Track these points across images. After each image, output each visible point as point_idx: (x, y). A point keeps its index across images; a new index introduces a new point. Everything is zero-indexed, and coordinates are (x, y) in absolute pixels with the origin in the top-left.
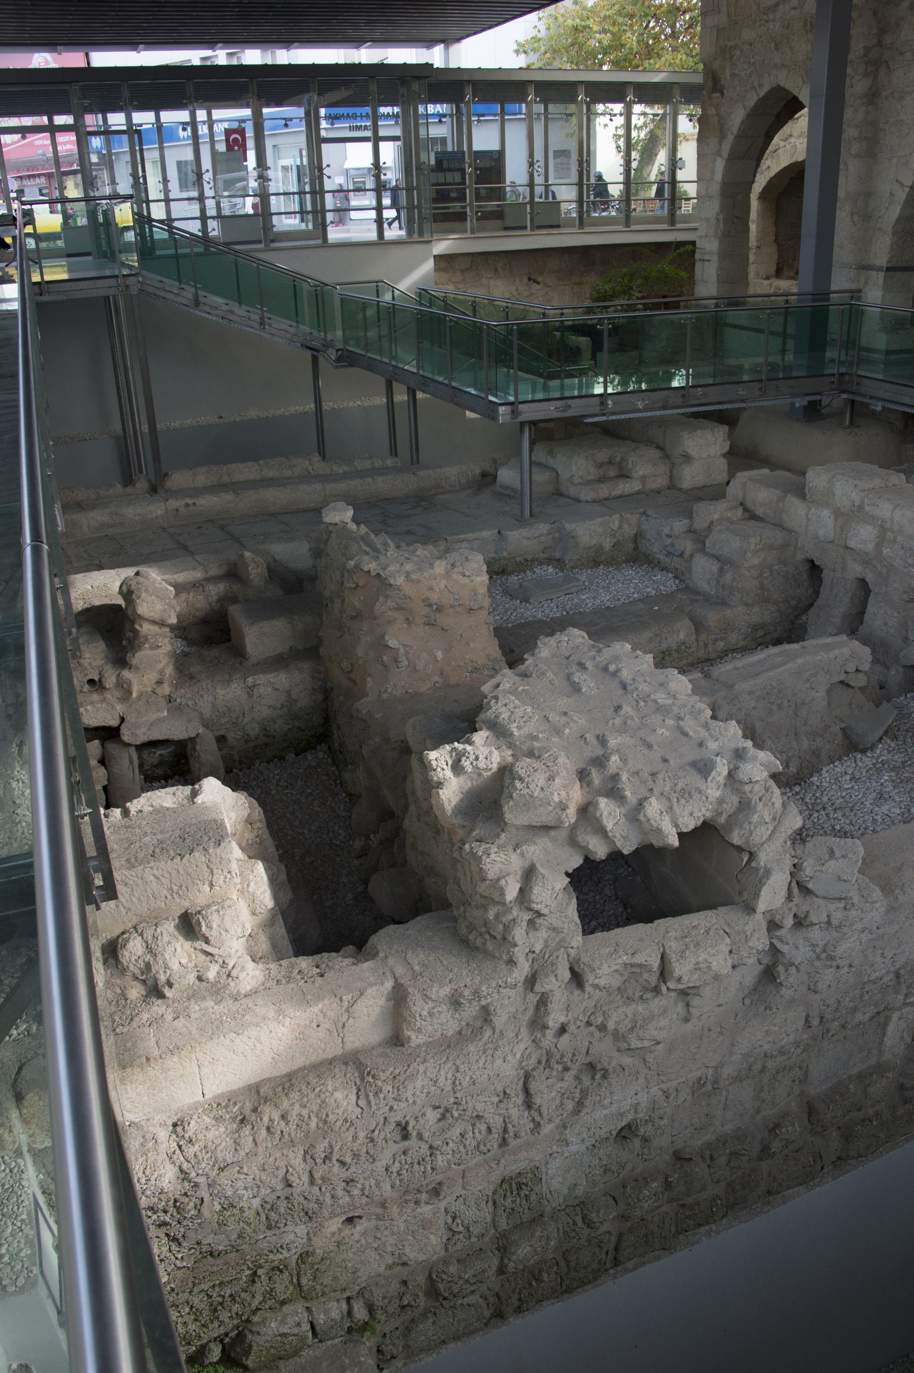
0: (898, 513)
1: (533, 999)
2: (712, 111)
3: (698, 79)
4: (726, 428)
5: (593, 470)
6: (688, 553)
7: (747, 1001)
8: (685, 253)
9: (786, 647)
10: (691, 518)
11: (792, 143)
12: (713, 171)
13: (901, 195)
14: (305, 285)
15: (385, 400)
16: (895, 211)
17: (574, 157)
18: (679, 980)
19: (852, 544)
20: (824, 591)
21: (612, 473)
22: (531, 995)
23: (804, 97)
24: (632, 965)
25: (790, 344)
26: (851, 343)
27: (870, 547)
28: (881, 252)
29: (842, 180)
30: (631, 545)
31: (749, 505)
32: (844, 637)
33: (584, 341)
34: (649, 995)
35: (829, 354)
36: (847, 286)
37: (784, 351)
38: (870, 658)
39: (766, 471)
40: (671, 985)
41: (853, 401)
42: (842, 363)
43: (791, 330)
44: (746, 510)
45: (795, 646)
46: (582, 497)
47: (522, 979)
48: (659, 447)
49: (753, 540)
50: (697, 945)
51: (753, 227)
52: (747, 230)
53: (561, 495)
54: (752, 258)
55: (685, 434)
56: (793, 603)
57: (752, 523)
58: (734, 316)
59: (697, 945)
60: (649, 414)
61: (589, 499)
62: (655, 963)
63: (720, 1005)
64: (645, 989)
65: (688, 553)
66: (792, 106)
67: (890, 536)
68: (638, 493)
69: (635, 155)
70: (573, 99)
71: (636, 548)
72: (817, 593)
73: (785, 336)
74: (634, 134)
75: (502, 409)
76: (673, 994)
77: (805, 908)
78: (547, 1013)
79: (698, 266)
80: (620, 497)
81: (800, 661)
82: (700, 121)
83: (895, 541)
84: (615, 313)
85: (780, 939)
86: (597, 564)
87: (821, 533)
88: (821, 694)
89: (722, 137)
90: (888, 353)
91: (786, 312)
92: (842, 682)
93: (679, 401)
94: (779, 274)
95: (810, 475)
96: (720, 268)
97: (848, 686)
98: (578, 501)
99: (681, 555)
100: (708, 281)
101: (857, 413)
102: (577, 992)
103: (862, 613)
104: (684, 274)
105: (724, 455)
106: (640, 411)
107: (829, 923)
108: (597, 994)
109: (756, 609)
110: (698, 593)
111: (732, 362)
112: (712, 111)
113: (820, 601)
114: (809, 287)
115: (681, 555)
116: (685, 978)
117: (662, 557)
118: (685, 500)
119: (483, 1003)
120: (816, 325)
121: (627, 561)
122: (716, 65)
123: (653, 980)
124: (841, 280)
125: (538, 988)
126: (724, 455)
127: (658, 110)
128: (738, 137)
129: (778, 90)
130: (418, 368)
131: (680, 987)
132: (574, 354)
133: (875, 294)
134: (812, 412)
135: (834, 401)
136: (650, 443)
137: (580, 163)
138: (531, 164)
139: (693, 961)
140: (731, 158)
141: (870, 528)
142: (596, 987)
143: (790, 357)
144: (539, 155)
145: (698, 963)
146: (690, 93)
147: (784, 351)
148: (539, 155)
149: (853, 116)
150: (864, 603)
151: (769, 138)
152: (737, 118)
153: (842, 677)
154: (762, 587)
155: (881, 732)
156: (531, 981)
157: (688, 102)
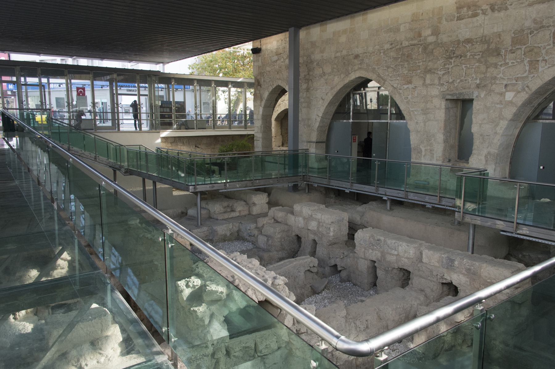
0: (323, 216)
1: (214, 361)
2: (258, 92)
3: (253, 81)
4: (267, 194)
5: (222, 209)
6: (256, 235)
7: (284, 363)
8: (251, 138)
9: (290, 259)
10: (256, 223)
11: (284, 103)
12: (259, 112)
13: (319, 119)
14: (112, 146)
15: (142, 189)
16: (317, 125)
17: (211, 105)
18: (261, 352)
19: (310, 228)
20: (302, 245)
21: (229, 210)
22: (213, 360)
23: (287, 89)
24: (246, 348)
25: (287, 167)
26: (306, 166)
27: (315, 228)
28: (314, 138)
29: (300, 115)
30: (236, 234)
31: (276, 218)
32: (309, 256)
33: (216, 168)
34: (252, 358)
35: (300, 170)
36: (304, 148)
37: (285, 169)
38: (317, 262)
39: (281, 207)
40: (259, 354)
41: (308, 184)
42: (304, 173)
43: (287, 163)
44: (275, 220)
45: (293, 259)
46: (219, 218)
47: (211, 353)
48: (244, 201)
49: (277, 229)
50: (266, 339)
51: (273, 130)
52: (271, 130)
53: (211, 218)
54: (273, 140)
55: (253, 196)
56: (293, 250)
57: (277, 224)
58: (267, 159)
59: (266, 339)
60: (241, 189)
61: (221, 219)
62: (253, 346)
63: (275, 364)
64: (250, 357)
65: (256, 235)
66: (283, 92)
67: (321, 224)
68: (238, 216)
69: (232, 105)
70: (210, 86)
71: (238, 235)
72: (300, 246)
73: (285, 164)
74: (231, 98)
75: (191, 187)
76: (260, 358)
77: (299, 327)
78: (219, 365)
79: (255, 142)
80: (232, 218)
81: (294, 263)
82: (254, 95)
83: (323, 226)
84: (227, 157)
85: (292, 339)
86: (225, 241)
87: (300, 225)
88: (303, 273)
89: (262, 100)
90: (318, 169)
91: (285, 156)
92: (309, 270)
93: (251, 185)
94: (283, 145)
95: (295, 207)
96: (263, 143)
97: (312, 272)
98: (217, 220)
99: (254, 236)
100: (259, 146)
101: (310, 188)
102: (228, 359)
103: (315, 252)
104: (250, 145)
105: (267, 203)
106: (237, 188)
107: (307, 332)
108: (235, 359)
109: (280, 253)
110: (261, 249)
111: (268, 172)
112: (258, 92)
113: (301, 248)
114: (292, 148)
115: (254, 236)
116: (263, 351)
117: (247, 237)
118: (254, 218)
119: (198, 362)
120: (295, 160)
121: (235, 239)
122: (259, 78)
123: (252, 352)
124: (302, 146)
125: (216, 357)
126: (267, 203)
127: (239, 90)
128: (267, 100)
129: (278, 86)
130: (158, 174)
131: (262, 355)
132: (214, 172)
133: (313, 150)
134: (295, 188)
135: (302, 184)
136: (241, 199)
137: (213, 107)
138: (196, 107)
139: (265, 344)
140: (265, 107)
141: (315, 222)
142: (234, 356)
143: (287, 171)
144: (198, 104)
145: (266, 345)
146: (250, 85)
147: (285, 169)
148: (198, 104)
149: (302, 95)
150: (316, 248)
151: (277, 101)
152: (266, 95)
153: (309, 268)
154: (282, 245)
155: (323, 287)
156: (213, 355)
157: (250, 88)
